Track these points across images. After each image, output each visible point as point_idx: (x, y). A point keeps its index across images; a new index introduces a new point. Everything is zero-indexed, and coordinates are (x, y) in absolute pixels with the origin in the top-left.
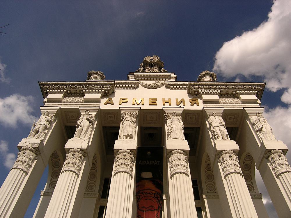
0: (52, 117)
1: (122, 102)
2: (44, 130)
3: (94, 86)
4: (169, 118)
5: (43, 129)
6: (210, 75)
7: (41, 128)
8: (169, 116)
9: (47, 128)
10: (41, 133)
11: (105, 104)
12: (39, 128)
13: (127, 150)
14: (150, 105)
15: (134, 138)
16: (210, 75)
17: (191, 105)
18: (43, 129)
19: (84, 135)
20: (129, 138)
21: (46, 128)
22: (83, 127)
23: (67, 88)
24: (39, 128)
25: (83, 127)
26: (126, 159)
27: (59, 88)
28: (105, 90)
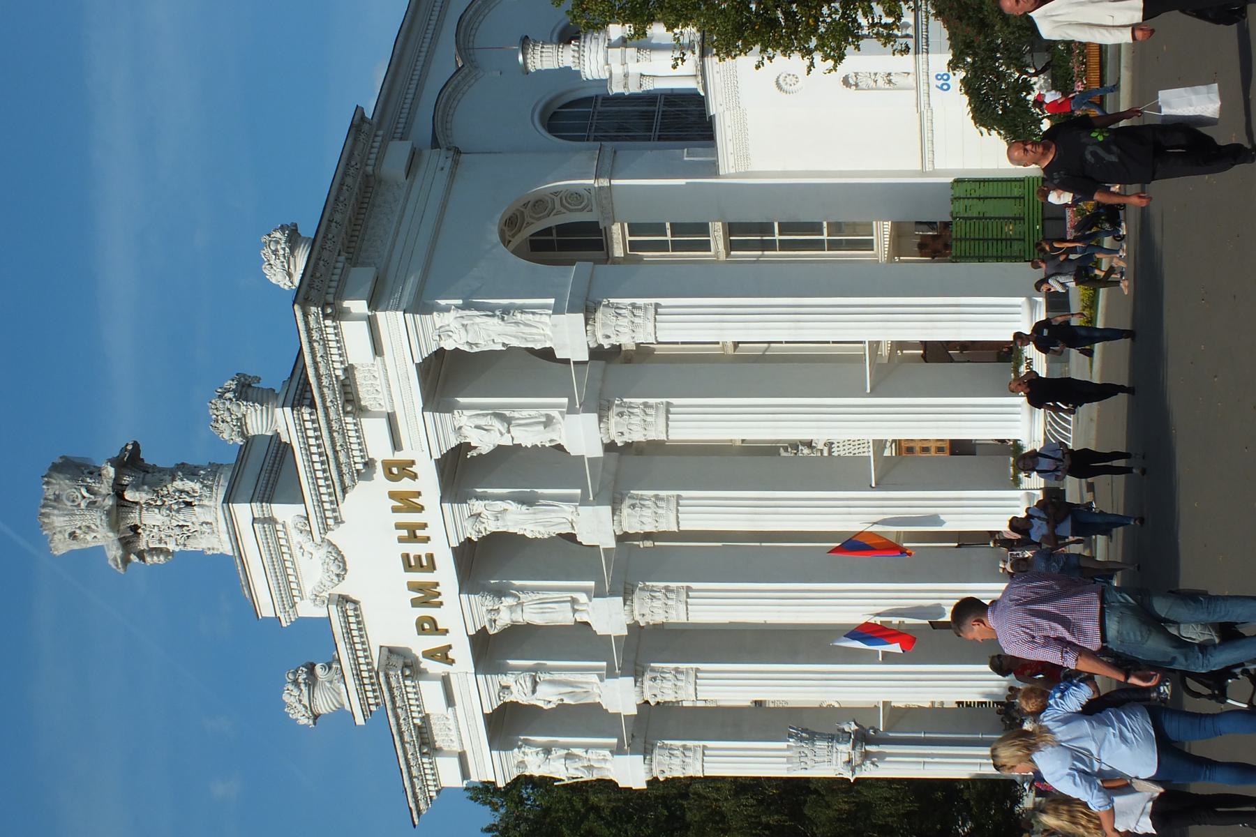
0: (524, 753)
1: (437, 629)
2: (579, 757)
3: (399, 707)
4: (485, 529)
5: (577, 760)
6: (241, 423)
7: (579, 765)
8: (480, 532)
9: (567, 754)
10: (589, 760)
11: (452, 662)
12: (577, 769)
13: (627, 612)
14: (434, 568)
15: (575, 595)
16: (241, 423)
17: (414, 476)
18: (577, 760)
19: (584, 686)
20: (576, 607)
21: (569, 757)
22: (560, 694)
23: (418, 759)
24: (577, 769)
25: (560, 694)
26: (652, 612)
27: (421, 775)
28: (405, 677)
